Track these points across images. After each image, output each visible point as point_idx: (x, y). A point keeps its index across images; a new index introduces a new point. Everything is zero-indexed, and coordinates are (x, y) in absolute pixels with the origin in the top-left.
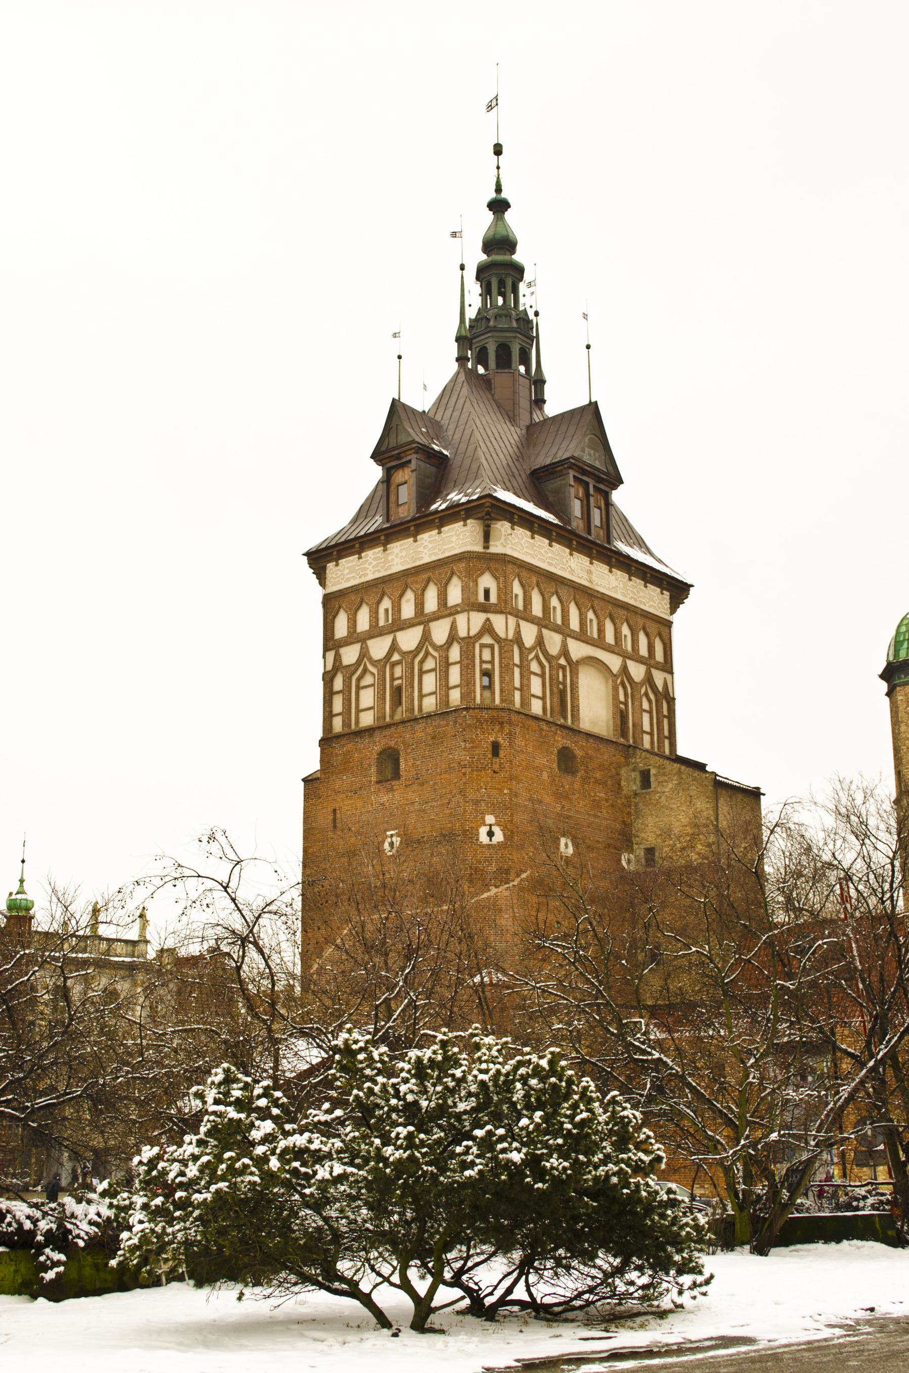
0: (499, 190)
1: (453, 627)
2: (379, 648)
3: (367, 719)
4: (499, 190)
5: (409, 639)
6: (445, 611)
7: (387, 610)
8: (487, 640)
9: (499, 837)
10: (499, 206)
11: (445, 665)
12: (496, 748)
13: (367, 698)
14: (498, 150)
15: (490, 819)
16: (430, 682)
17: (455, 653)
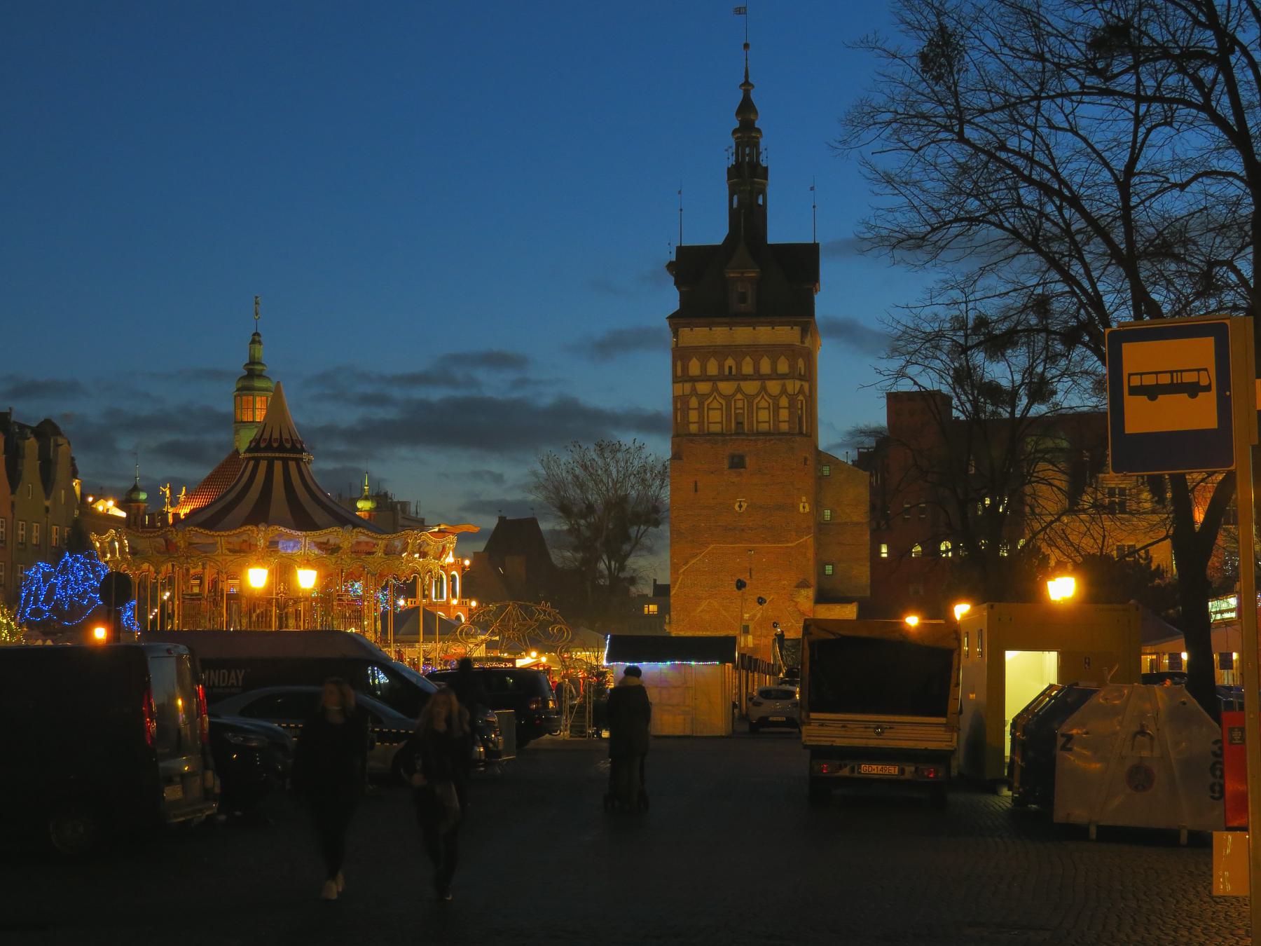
0: (747, 76)
1: (784, 386)
2: (726, 387)
3: (715, 428)
4: (747, 76)
5: (751, 387)
6: (775, 376)
7: (730, 368)
8: (801, 397)
9: (807, 509)
10: (747, 85)
11: (777, 408)
12: (806, 459)
13: (715, 416)
14: (746, 46)
15: (804, 499)
16: (764, 415)
17: (784, 402)
